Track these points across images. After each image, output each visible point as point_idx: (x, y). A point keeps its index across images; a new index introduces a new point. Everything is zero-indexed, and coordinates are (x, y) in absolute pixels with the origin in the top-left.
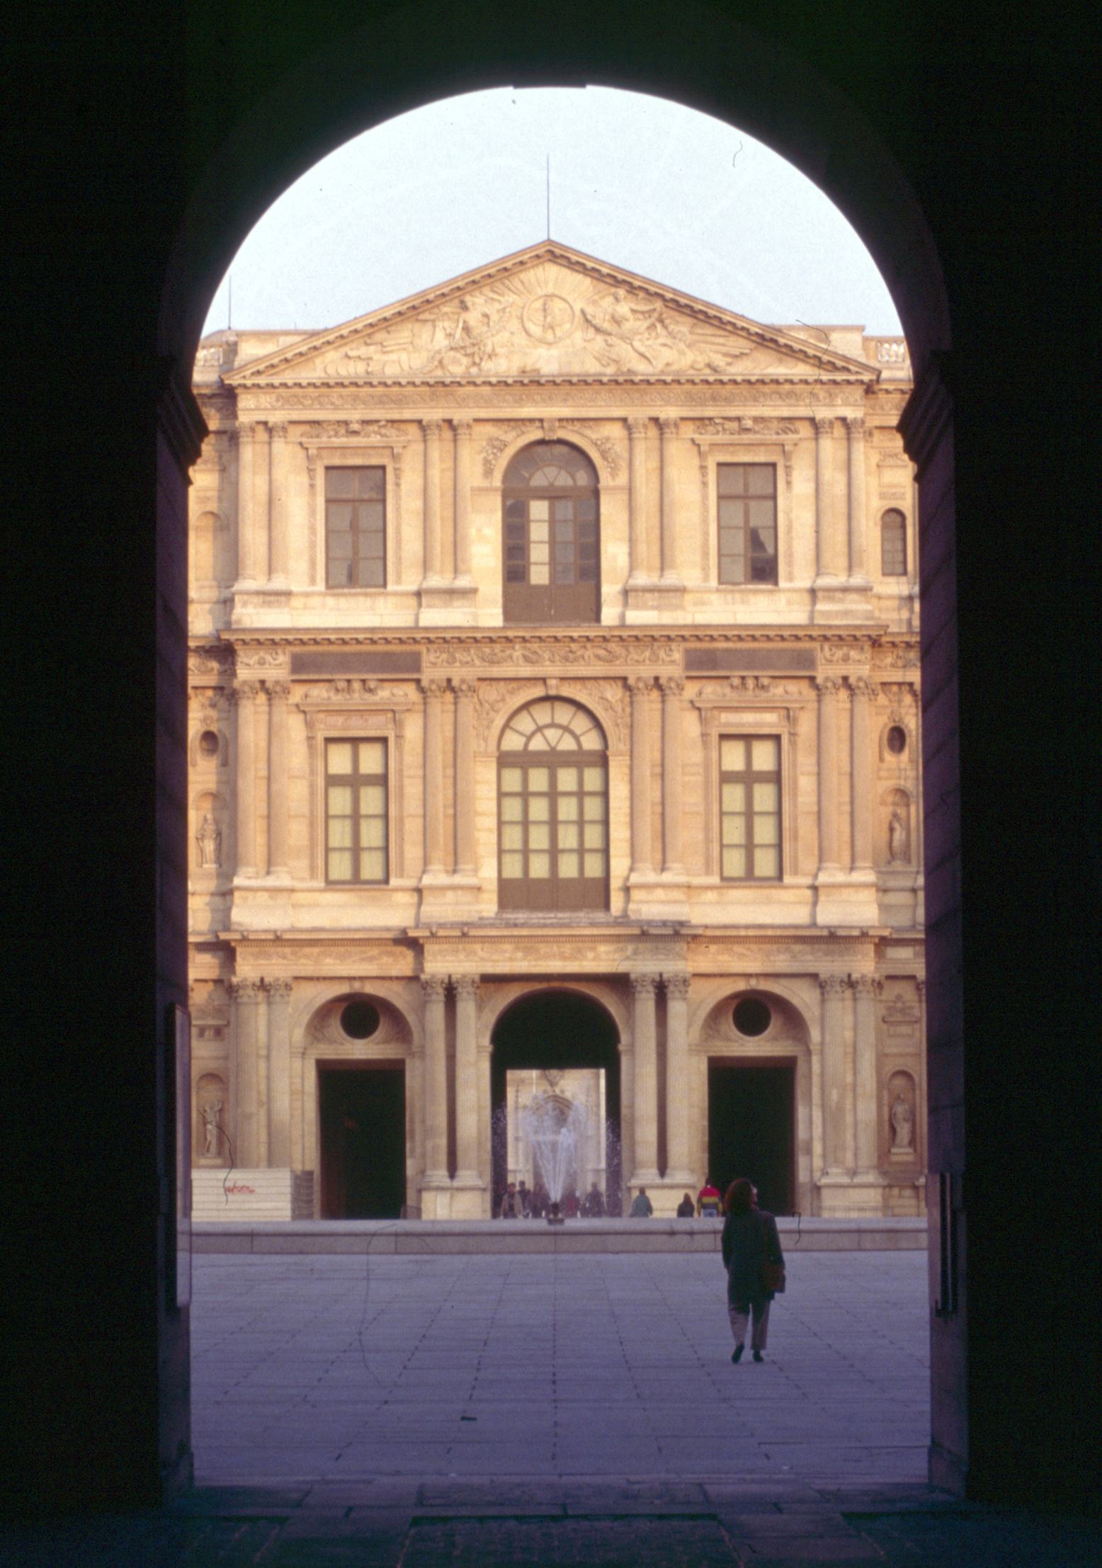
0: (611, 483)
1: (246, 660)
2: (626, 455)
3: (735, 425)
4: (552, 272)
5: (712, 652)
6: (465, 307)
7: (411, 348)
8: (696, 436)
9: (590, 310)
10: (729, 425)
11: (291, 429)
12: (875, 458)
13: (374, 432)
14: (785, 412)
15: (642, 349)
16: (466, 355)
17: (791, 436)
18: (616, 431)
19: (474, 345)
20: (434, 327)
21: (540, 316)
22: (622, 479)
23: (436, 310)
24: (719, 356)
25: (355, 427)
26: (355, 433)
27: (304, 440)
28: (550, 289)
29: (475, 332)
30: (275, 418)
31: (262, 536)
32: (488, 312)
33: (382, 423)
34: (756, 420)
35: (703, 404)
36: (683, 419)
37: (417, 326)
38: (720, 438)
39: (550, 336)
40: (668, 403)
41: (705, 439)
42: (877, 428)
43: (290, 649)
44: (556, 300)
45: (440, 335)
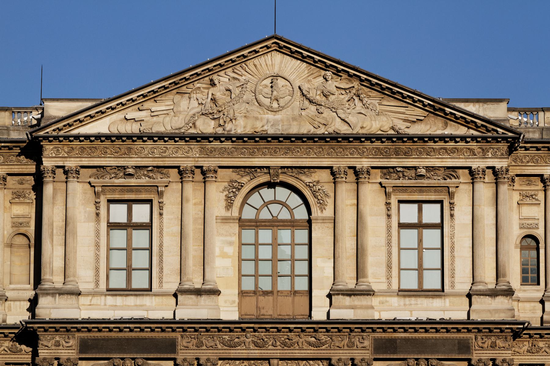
0: (320, 214)
1: (45, 343)
2: (332, 195)
3: (412, 173)
4: (277, 62)
5: (393, 341)
6: (213, 84)
7: (172, 114)
8: (383, 181)
9: (305, 88)
10: (408, 173)
11: (82, 171)
12: (516, 197)
13: (144, 175)
14: (450, 163)
15: (343, 116)
16: (214, 119)
17: (454, 180)
18: (325, 175)
19: (220, 112)
20: (190, 98)
21: (268, 90)
22: (329, 212)
23: (191, 86)
24: (401, 122)
25: (131, 171)
26: (130, 175)
27: (92, 180)
28: (276, 71)
29: (220, 103)
30: (71, 163)
31: (59, 251)
32: (231, 88)
33: (150, 168)
34: (428, 168)
35: (388, 156)
36: (373, 168)
37: (178, 97)
38: (399, 182)
39: (275, 105)
40: (362, 155)
41: (390, 182)
42: (517, 175)
43: (77, 335)
44: (279, 78)
45: (194, 103)
